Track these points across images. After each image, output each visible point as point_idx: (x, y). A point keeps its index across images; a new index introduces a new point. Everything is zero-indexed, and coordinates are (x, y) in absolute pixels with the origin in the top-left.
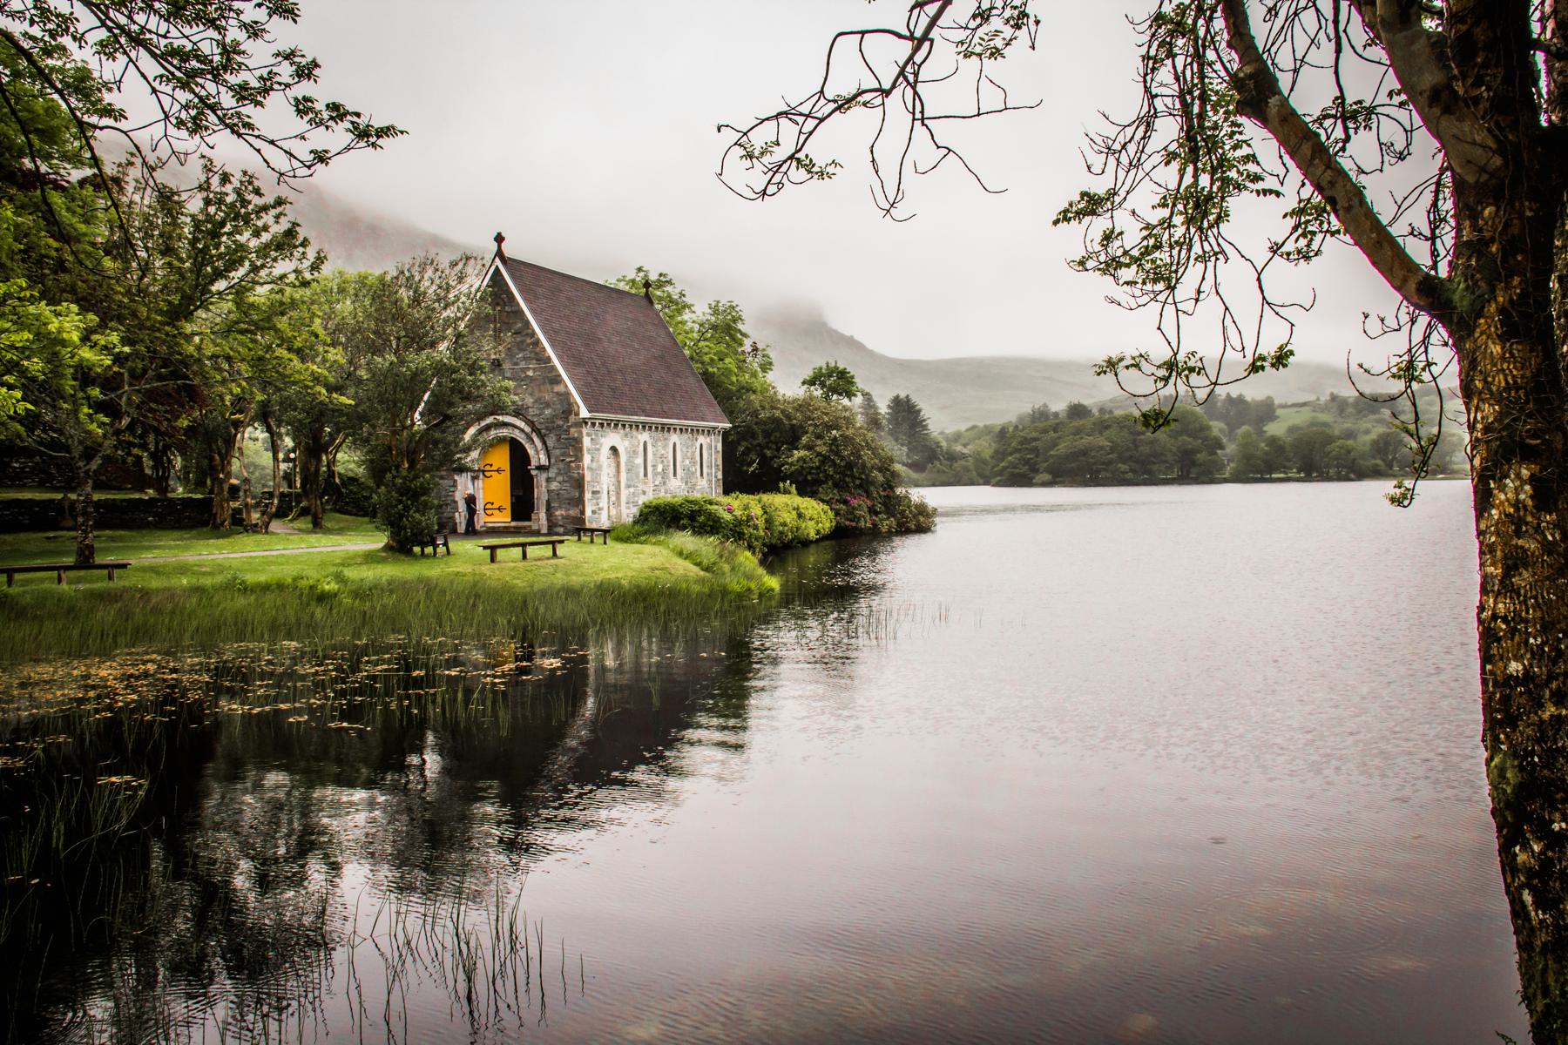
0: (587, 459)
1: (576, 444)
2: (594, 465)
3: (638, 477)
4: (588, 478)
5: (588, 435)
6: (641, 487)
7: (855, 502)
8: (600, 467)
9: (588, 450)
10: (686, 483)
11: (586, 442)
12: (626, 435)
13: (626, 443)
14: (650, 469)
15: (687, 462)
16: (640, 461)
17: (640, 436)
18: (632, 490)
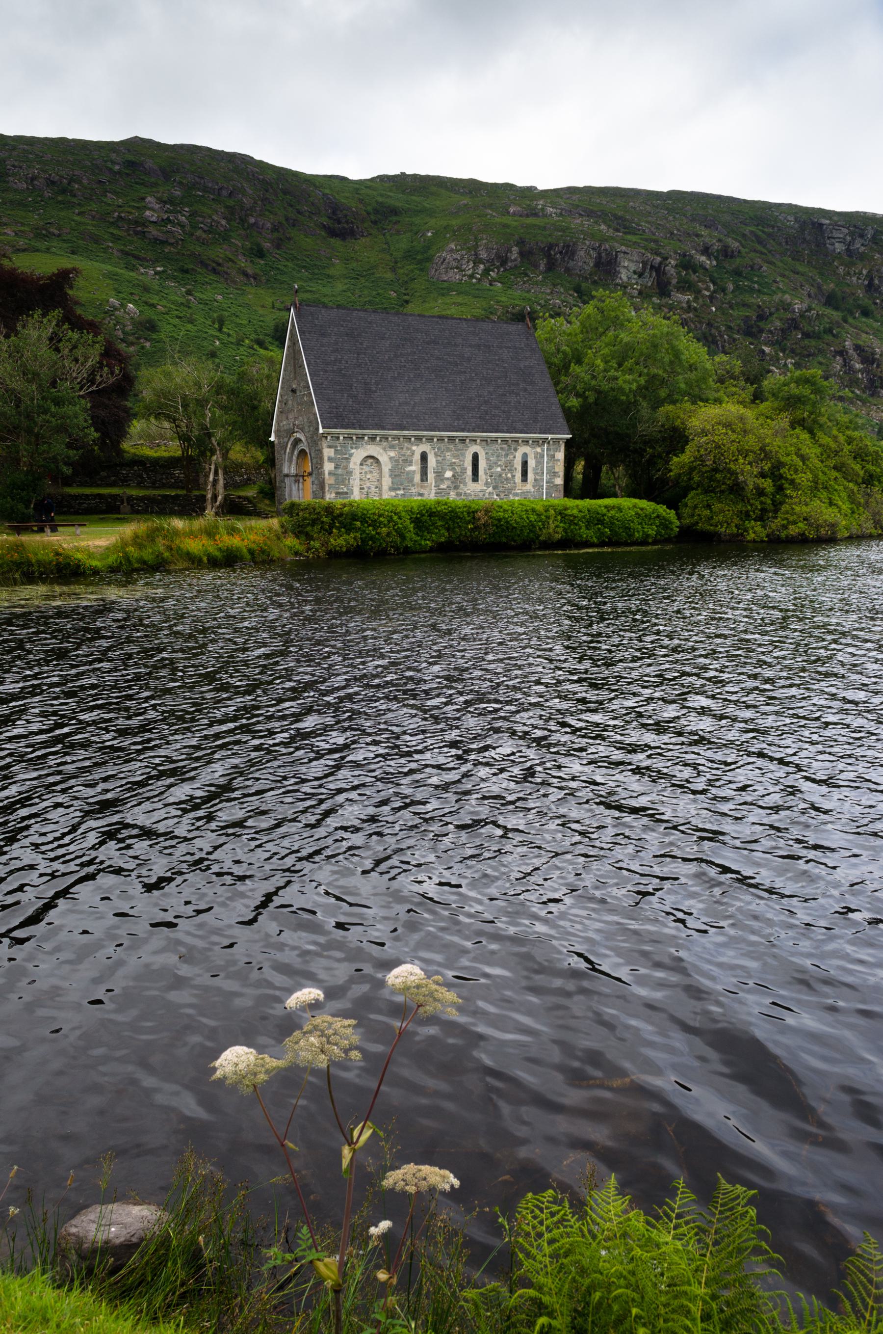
0: (328, 467)
1: (320, 451)
2: (340, 471)
3: (411, 480)
4: (329, 480)
5: (329, 447)
6: (414, 490)
7: (717, 506)
8: (350, 473)
9: (330, 459)
10: (494, 488)
11: (328, 452)
12: (392, 447)
13: (392, 454)
14: (431, 476)
15: (499, 469)
16: (415, 467)
17: (414, 448)
18: (402, 492)
